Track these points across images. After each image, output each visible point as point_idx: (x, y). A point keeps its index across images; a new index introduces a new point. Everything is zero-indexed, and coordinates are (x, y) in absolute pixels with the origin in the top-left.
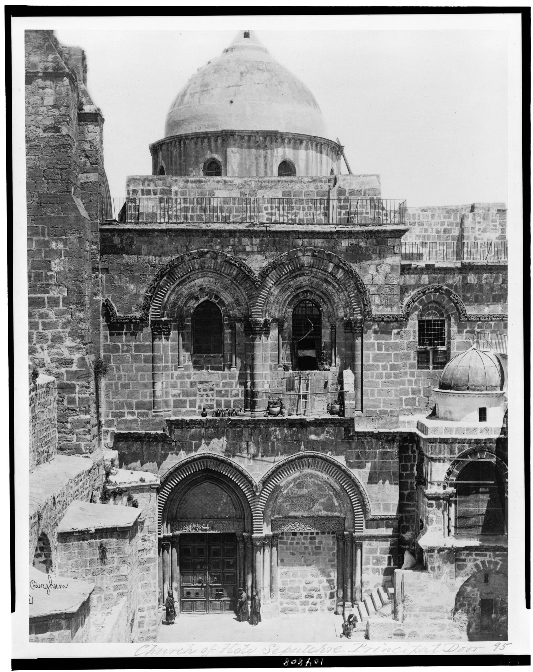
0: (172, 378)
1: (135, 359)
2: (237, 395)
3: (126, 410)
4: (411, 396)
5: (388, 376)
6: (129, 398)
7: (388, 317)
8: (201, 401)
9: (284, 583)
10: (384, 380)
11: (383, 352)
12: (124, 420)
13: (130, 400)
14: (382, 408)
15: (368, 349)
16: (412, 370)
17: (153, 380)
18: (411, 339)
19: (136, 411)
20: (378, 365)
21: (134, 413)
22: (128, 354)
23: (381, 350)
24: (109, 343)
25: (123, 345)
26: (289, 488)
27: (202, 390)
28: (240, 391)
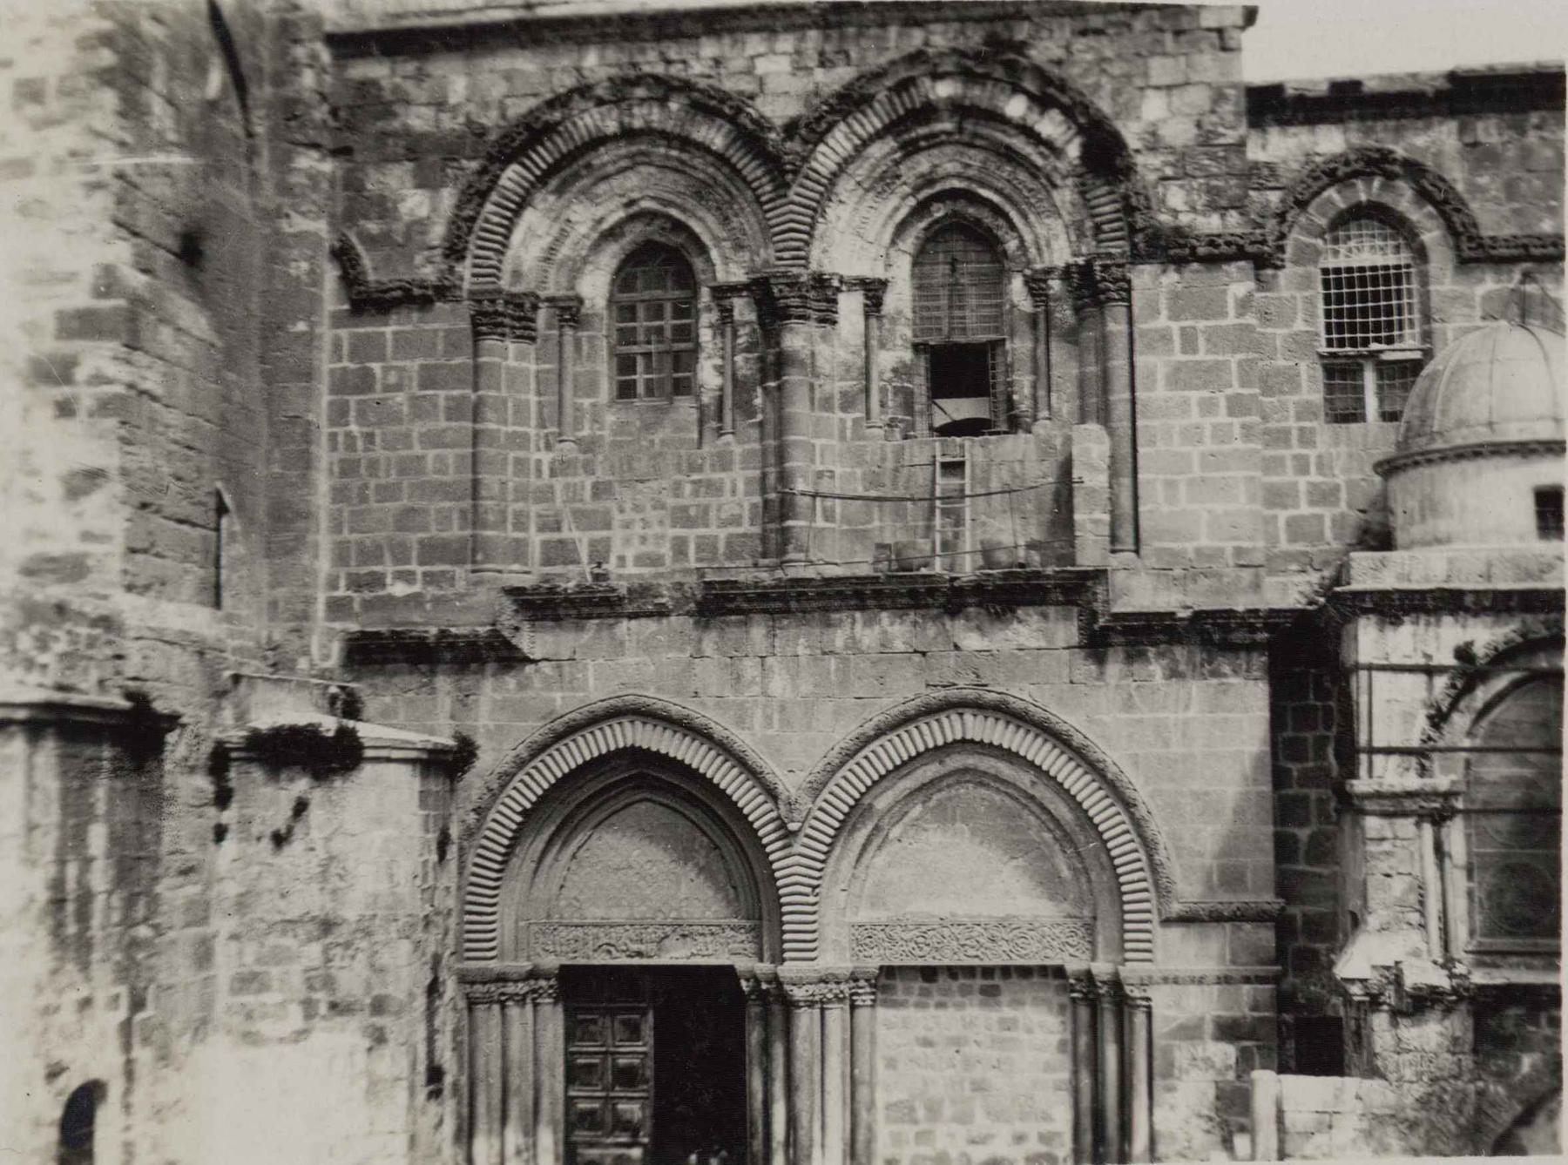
0: (539, 472)
1: (420, 409)
2: (736, 520)
3: (388, 568)
4: (1305, 509)
5: (1221, 434)
6: (400, 529)
7: (1212, 243)
8: (627, 541)
9: (897, 1140)
10: (1209, 446)
11: (1201, 356)
12: (379, 598)
13: (400, 536)
14: (1204, 542)
15: (1150, 348)
16: (1307, 424)
17: (475, 472)
18: (1299, 325)
19: (420, 570)
20: (1186, 402)
21: (412, 573)
22: (400, 397)
23: (1195, 351)
24: (346, 363)
25: (386, 370)
26: (906, 820)
27: (628, 506)
28: (747, 506)
